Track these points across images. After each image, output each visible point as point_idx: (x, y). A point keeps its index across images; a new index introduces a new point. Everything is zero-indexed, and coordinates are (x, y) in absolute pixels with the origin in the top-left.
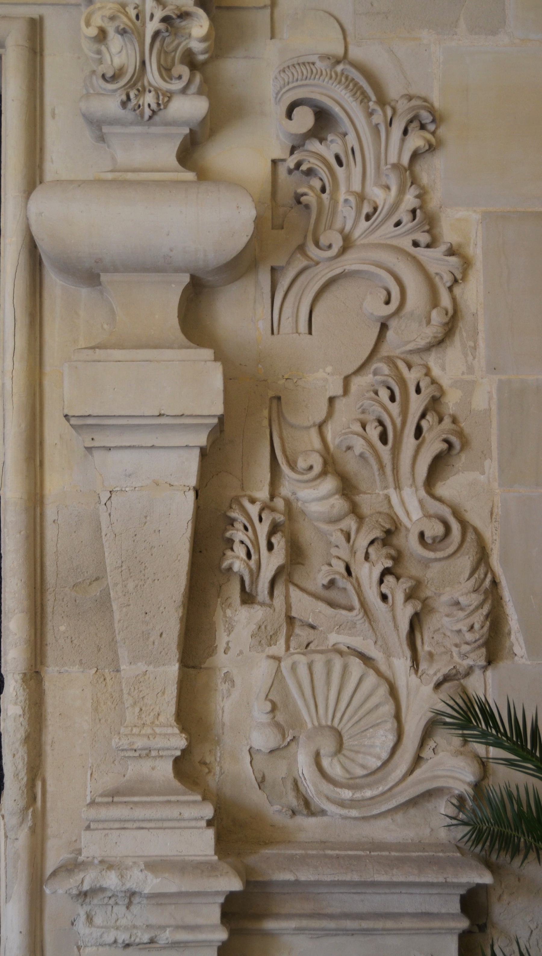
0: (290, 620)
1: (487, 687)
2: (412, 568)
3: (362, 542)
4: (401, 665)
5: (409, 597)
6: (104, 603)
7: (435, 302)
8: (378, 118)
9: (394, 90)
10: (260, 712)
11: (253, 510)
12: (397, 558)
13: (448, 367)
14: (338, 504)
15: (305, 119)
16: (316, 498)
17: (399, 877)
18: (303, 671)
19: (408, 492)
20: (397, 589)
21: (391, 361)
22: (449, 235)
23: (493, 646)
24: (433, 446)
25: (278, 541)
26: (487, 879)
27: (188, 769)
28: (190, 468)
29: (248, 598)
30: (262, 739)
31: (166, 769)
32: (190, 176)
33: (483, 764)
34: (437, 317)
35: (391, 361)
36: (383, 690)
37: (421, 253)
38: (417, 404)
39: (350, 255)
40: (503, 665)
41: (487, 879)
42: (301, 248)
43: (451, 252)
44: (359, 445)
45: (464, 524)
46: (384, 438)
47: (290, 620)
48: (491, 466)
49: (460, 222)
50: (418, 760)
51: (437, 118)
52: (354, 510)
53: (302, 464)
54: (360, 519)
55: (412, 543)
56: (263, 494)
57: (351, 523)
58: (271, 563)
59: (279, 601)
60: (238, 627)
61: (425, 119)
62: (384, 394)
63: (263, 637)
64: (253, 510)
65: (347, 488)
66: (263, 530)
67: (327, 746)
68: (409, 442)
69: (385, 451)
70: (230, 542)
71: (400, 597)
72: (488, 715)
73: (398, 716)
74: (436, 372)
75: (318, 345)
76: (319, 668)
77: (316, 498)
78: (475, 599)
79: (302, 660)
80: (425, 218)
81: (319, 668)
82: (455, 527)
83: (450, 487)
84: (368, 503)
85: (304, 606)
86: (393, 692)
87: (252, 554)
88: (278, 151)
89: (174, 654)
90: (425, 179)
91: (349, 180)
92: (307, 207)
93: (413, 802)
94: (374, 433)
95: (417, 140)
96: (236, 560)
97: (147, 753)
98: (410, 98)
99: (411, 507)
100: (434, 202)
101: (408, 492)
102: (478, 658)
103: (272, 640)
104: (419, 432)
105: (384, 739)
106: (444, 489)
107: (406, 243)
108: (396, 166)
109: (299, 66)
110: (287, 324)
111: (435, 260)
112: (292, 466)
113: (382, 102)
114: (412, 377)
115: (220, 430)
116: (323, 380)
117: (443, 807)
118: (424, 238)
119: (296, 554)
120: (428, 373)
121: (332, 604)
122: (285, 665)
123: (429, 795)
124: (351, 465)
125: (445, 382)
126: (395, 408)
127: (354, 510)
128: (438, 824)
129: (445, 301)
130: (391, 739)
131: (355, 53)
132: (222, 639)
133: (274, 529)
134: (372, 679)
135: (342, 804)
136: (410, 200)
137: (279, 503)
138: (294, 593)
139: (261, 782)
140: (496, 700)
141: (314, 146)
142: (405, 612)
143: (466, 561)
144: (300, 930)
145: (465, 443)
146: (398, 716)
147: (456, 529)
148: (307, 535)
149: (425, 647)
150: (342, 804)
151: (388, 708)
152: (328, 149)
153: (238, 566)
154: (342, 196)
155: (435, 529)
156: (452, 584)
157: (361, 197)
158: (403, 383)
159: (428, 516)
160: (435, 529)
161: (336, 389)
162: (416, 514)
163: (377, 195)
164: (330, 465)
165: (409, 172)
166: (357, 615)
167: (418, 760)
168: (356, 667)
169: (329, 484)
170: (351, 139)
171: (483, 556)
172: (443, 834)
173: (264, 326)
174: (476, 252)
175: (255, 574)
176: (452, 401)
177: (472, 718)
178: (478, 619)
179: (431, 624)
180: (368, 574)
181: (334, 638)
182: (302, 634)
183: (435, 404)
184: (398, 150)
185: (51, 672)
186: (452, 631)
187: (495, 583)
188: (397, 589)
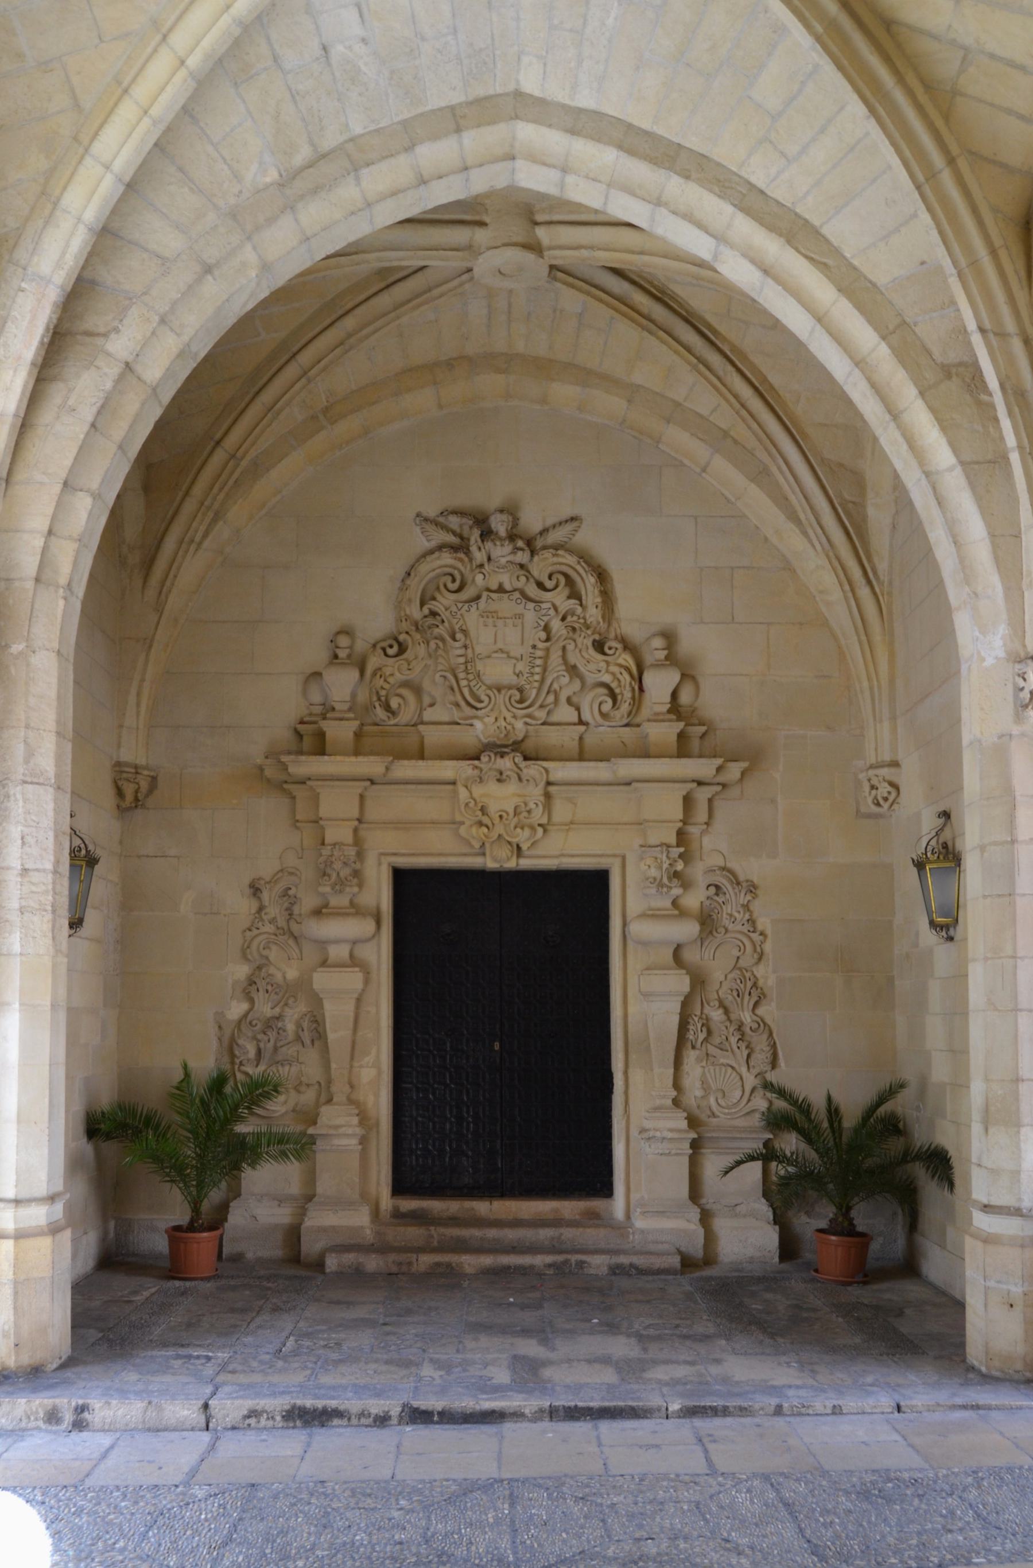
0: (707, 1054)
1: (772, 1077)
2: (747, 1038)
3: (731, 1030)
4: (744, 1069)
5: (747, 1047)
6: (648, 1049)
7: (755, 951)
8: (737, 890)
9: (742, 878)
10: (698, 1084)
11: (696, 1019)
12: (743, 1035)
13: (760, 971)
14: (724, 1017)
15: (713, 890)
16: (716, 1015)
17: (743, 1136)
18: (712, 1071)
19: (746, 1013)
20: (743, 1045)
21: (740, 969)
22: (760, 927)
23: (774, 1064)
24: (755, 999)
25: (704, 1029)
26: (771, 1136)
27: (676, 1103)
28: (677, 1008)
29: (693, 1047)
30: (699, 1093)
31: (669, 1102)
32: (676, 912)
33: (771, 1103)
34: (756, 956)
35: (740, 969)
36: (738, 1078)
37: (751, 935)
38: (749, 984)
39: (728, 935)
40: (777, 1070)
41: (771, 1136)
42: (711, 932)
43: (761, 934)
44: (730, 998)
45: (765, 1024)
46: (738, 995)
47: (707, 1054)
48: (774, 1004)
49: (763, 923)
50: (749, 1100)
51: (755, 887)
52: (729, 1019)
53: (712, 1004)
54: (731, 1022)
55: (747, 1030)
56: (698, 1013)
57: (728, 1024)
58: (702, 1036)
59: (704, 1048)
60: (691, 1057)
61: (752, 888)
62: (739, 981)
63: (699, 1060)
64: (696, 1019)
65: (727, 1012)
66: (699, 1026)
67: (720, 1095)
68: (747, 997)
69: (739, 1000)
70: (688, 1030)
71: (744, 1048)
72: (772, 1085)
73: (743, 1086)
74: (755, 973)
75: (718, 964)
76: (717, 1070)
77: (716, 1015)
78: (768, 1048)
79: (712, 1068)
80: (752, 921)
81: (717, 1070)
82: (762, 1025)
83: (761, 1011)
84: (733, 1016)
85: (712, 1050)
86: (741, 1078)
87: (696, 1033)
88: (703, 898)
89: (672, 1065)
90: (751, 908)
91: (727, 909)
92: (713, 920)
93: (748, 1113)
94: (735, 994)
95: (749, 897)
96: (691, 1036)
97: (664, 1097)
98: (747, 881)
99: (747, 1017)
100: (755, 915)
101: (746, 1013)
102: (769, 1068)
103: (702, 1061)
104: (750, 994)
105: (738, 1093)
106: (758, 1012)
107: (746, 931)
108: (743, 905)
109: (711, 871)
110: (706, 957)
111: (755, 936)
112: (708, 1004)
113: (738, 883)
114: (748, 975)
115: (686, 997)
116: (718, 975)
117: (757, 1116)
118: (752, 929)
119: (709, 1032)
120: (753, 974)
121: (722, 1049)
122: (706, 1070)
123: (753, 1111)
124: (727, 1003)
125: (758, 976)
126: (742, 986)
127: (729, 1019)
128: (756, 1120)
129: (759, 949)
130: (741, 1093)
131: (729, 865)
132: (685, 1061)
133: (703, 1025)
134: (734, 1074)
135: (725, 1114)
136: (747, 916)
137: (704, 1016)
138: (709, 1046)
139: (698, 1107)
140: (774, 1082)
141: (716, 898)
142: (745, 1053)
143: (765, 1036)
144: (713, 1153)
145: (765, 996)
146: (743, 1086)
147: (762, 1024)
148: (713, 1027)
149: (751, 1064)
150: (725, 1114)
151: (740, 1083)
152: (720, 899)
153: (691, 1037)
154: (725, 916)
155: (755, 1026)
156: (761, 1043)
157: (731, 915)
158: (745, 977)
159: (753, 1021)
160: (755, 1026)
161: (722, 978)
162: (749, 1020)
163: (736, 914)
164: (722, 1005)
165: (746, 907)
166: (730, 1053)
167: (749, 1100)
168: (730, 1070)
169: (721, 1011)
170: (728, 896)
171: (771, 1034)
172: (757, 1124)
173: (698, 957)
174: (769, 932)
175: (696, 1040)
176: (760, 983)
177: (767, 1086)
178: (769, 1055)
179: (753, 1056)
180: (733, 1040)
181: (722, 1061)
182: (711, 1059)
183: (755, 985)
184: (743, 899)
185: (630, 1070)
186: (761, 1058)
187: (775, 1043)
188: (743, 1045)
